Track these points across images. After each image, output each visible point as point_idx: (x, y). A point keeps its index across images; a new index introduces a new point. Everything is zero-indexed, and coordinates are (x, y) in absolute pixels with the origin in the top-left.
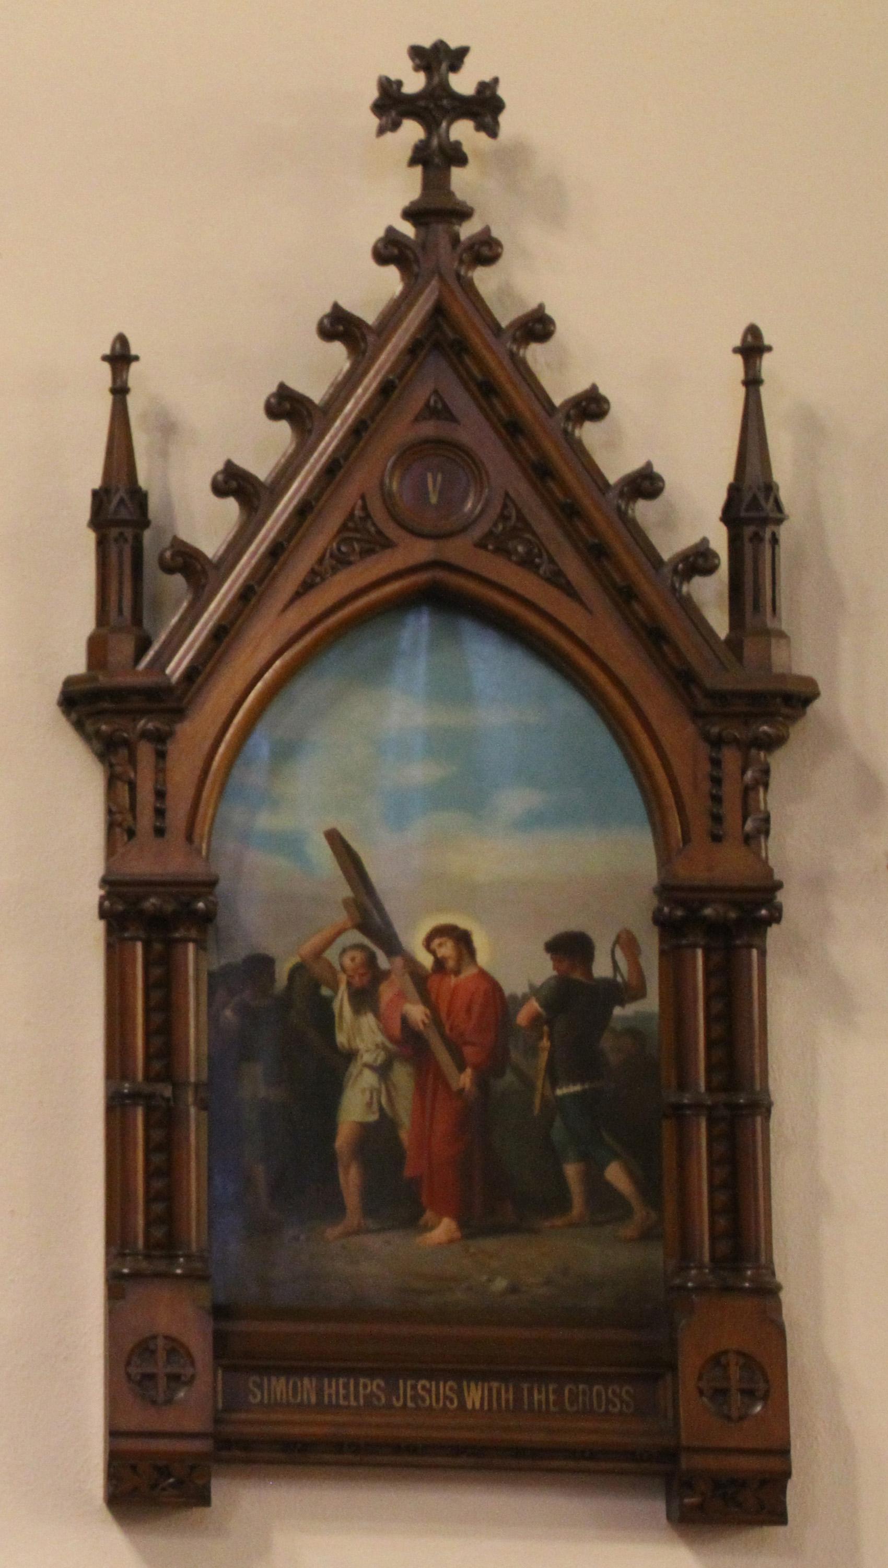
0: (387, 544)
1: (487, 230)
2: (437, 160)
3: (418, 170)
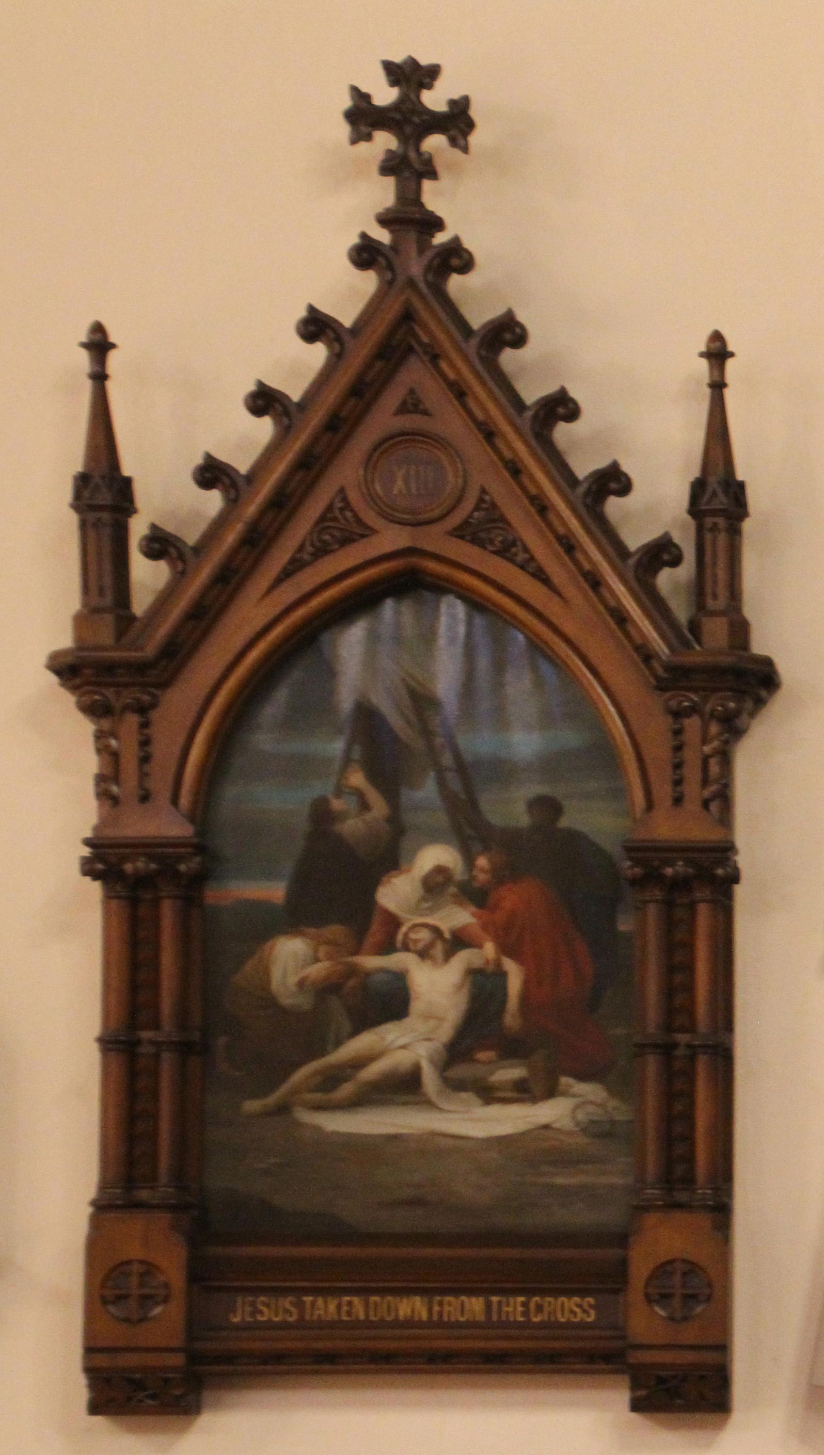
0: (367, 532)
1: (456, 240)
2: (409, 170)
3: (390, 182)
